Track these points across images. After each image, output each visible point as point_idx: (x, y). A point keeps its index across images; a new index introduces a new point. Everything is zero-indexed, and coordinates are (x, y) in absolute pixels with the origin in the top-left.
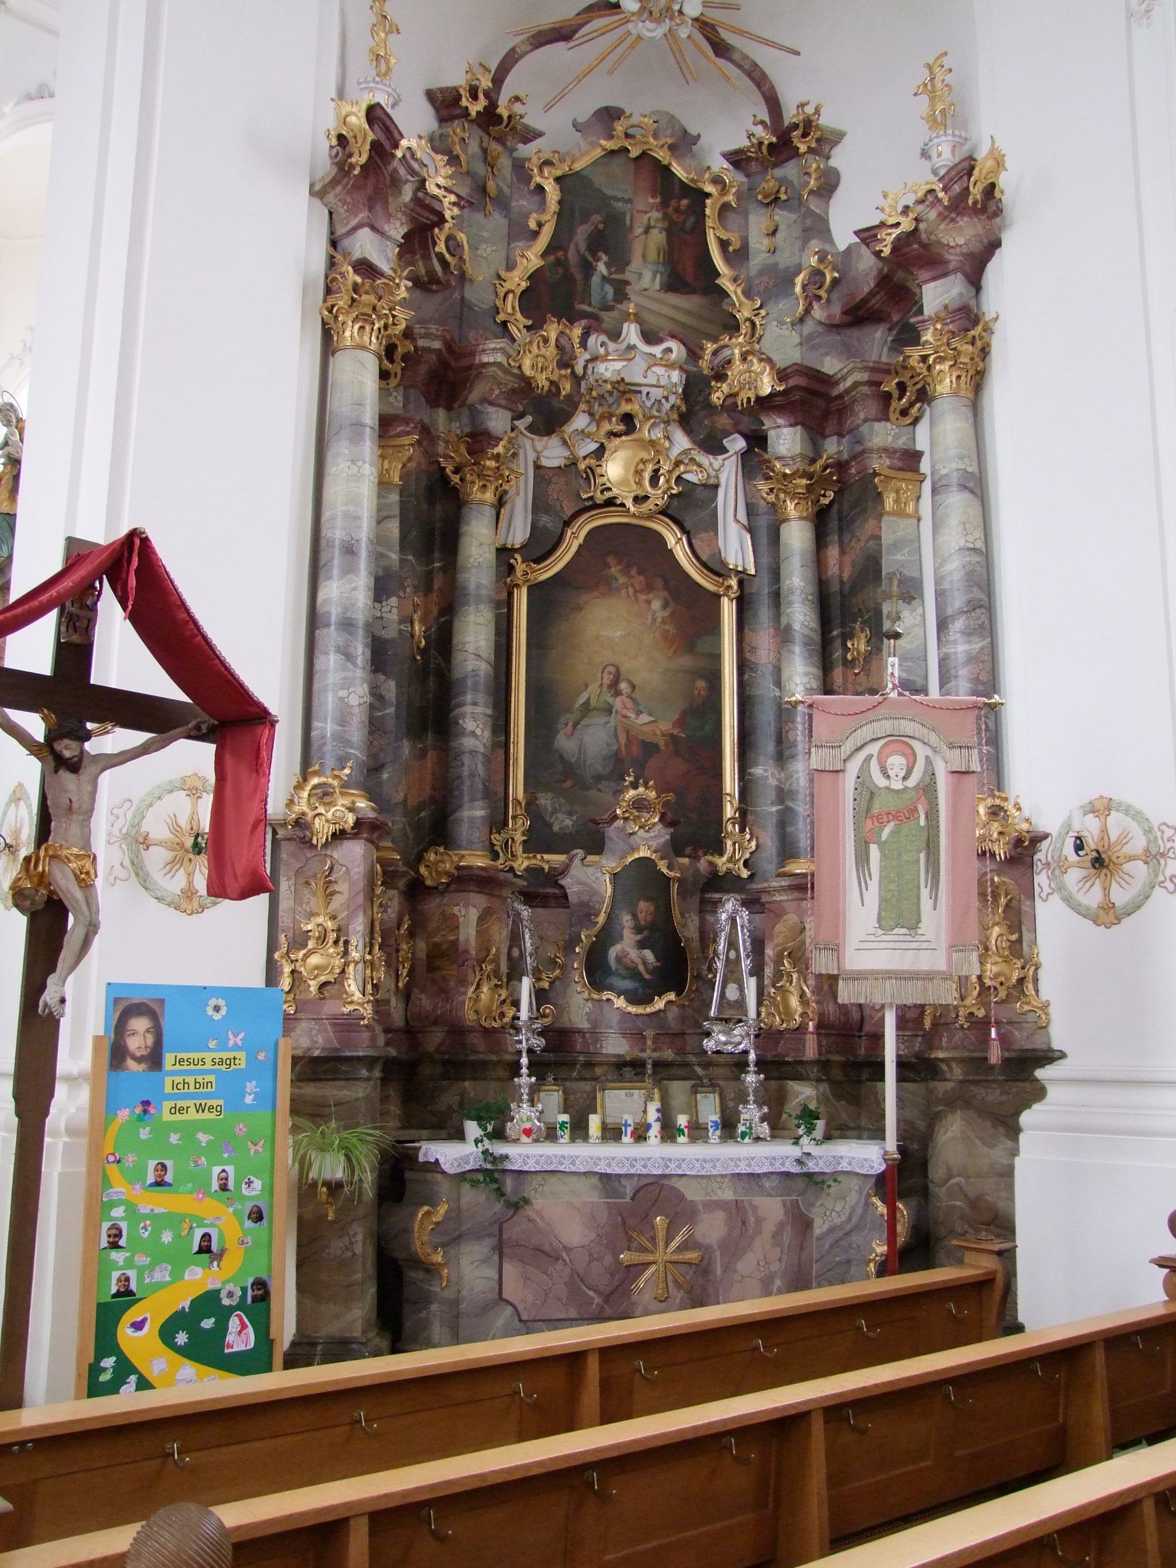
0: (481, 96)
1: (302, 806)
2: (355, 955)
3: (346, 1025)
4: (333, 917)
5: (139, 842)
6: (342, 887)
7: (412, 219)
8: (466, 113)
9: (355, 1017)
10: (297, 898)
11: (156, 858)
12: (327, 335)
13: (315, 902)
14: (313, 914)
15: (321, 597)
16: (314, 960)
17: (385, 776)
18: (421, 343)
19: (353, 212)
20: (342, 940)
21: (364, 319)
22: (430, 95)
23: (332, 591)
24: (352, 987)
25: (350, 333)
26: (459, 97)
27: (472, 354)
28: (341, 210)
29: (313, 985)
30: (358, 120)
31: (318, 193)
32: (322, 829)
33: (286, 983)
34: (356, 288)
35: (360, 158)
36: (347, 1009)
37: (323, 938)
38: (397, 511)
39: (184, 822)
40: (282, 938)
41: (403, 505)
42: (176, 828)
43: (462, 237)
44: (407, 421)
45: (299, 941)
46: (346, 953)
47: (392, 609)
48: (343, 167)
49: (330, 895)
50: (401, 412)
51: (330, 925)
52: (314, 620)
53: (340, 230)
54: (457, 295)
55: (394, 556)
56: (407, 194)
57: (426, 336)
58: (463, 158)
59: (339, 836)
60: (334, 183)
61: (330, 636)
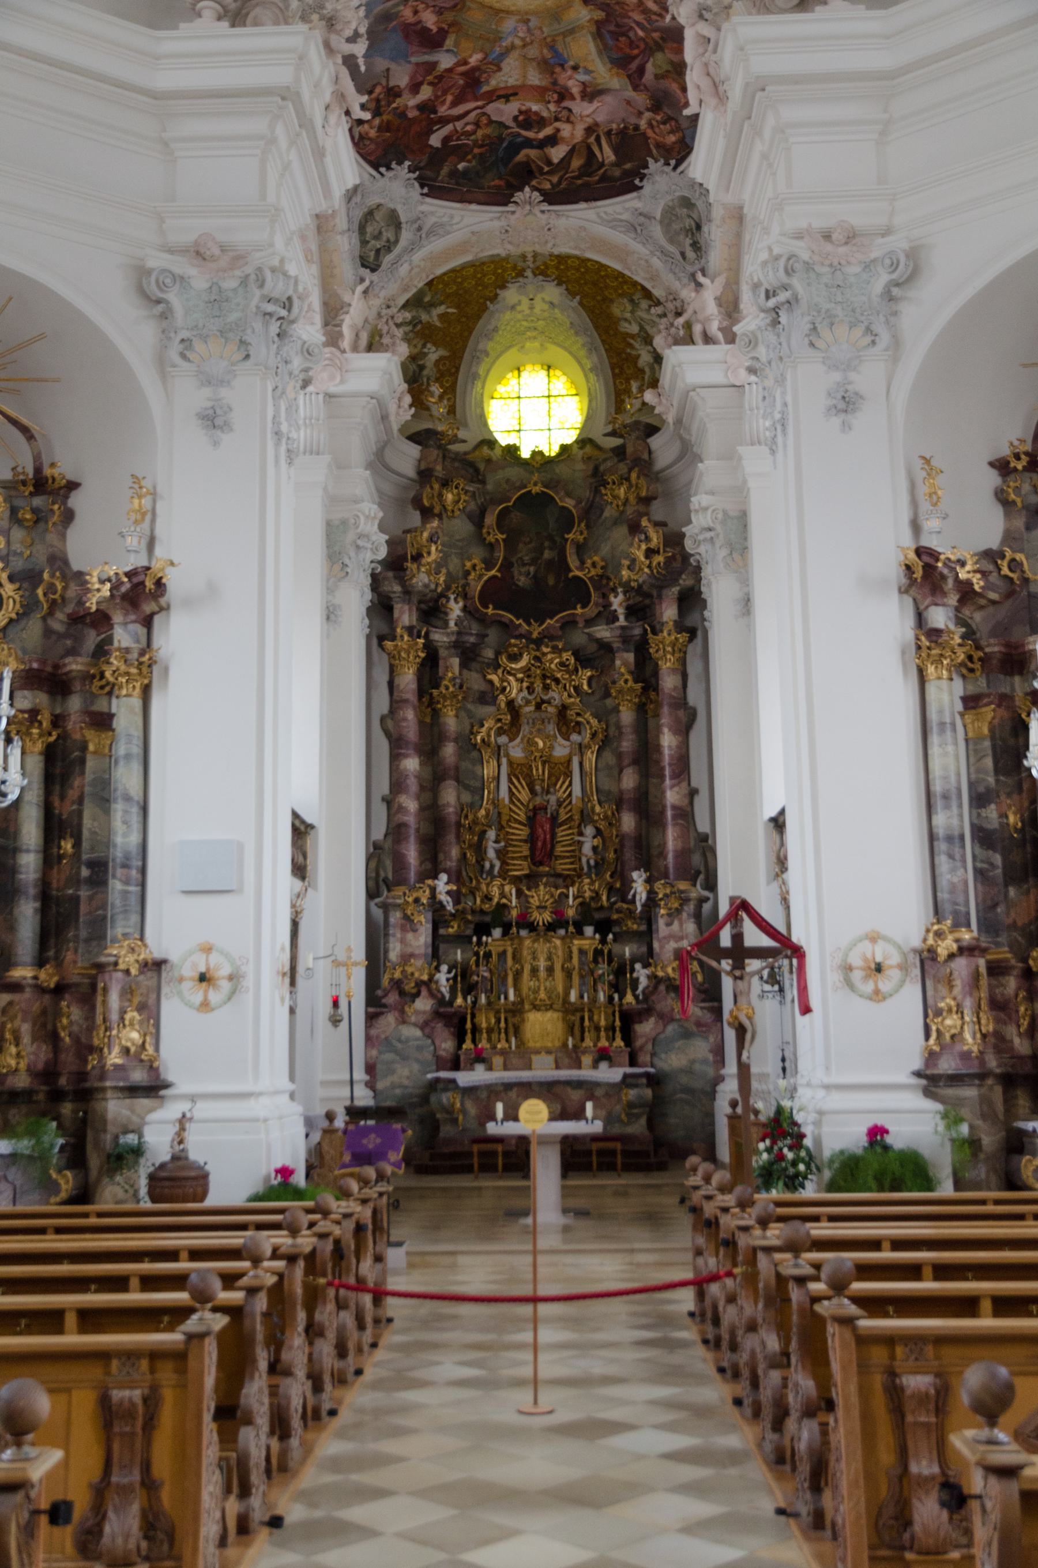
0: (1023, 457)
1: (930, 941)
2: (967, 1019)
3: (965, 1056)
4: (954, 999)
5: (848, 969)
6: (958, 983)
7: (959, 591)
8: (1015, 470)
9: (970, 1052)
10: (936, 990)
11: (857, 976)
12: (921, 672)
13: (943, 990)
14: (943, 998)
15: (934, 822)
16: (948, 1022)
17: (999, 910)
18: (987, 650)
19: (925, 597)
20: (960, 1011)
21: (938, 661)
22: (991, 464)
23: (940, 820)
24: (968, 1036)
25: (931, 669)
26: (1008, 463)
27: (1023, 645)
28: (919, 597)
29: (948, 1036)
30: (912, 555)
31: (903, 591)
32: (942, 952)
33: (934, 1035)
34: (929, 648)
35: (919, 574)
36: (966, 1048)
37: (950, 1011)
38: (990, 752)
39: (869, 956)
40: (930, 1012)
41: (994, 747)
42: (866, 960)
43: (1019, 557)
44: (988, 695)
45: (939, 1013)
46: (962, 1018)
47: (991, 813)
48: (912, 582)
49: (951, 987)
50: (986, 691)
51: (953, 1003)
52: (932, 837)
53: (922, 607)
54: (1025, 593)
55: (991, 780)
56: (950, 582)
57: (989, 645)
58: (1018, 501)
59: (951, 956)
60: (910, 586)
61: (942, 846)
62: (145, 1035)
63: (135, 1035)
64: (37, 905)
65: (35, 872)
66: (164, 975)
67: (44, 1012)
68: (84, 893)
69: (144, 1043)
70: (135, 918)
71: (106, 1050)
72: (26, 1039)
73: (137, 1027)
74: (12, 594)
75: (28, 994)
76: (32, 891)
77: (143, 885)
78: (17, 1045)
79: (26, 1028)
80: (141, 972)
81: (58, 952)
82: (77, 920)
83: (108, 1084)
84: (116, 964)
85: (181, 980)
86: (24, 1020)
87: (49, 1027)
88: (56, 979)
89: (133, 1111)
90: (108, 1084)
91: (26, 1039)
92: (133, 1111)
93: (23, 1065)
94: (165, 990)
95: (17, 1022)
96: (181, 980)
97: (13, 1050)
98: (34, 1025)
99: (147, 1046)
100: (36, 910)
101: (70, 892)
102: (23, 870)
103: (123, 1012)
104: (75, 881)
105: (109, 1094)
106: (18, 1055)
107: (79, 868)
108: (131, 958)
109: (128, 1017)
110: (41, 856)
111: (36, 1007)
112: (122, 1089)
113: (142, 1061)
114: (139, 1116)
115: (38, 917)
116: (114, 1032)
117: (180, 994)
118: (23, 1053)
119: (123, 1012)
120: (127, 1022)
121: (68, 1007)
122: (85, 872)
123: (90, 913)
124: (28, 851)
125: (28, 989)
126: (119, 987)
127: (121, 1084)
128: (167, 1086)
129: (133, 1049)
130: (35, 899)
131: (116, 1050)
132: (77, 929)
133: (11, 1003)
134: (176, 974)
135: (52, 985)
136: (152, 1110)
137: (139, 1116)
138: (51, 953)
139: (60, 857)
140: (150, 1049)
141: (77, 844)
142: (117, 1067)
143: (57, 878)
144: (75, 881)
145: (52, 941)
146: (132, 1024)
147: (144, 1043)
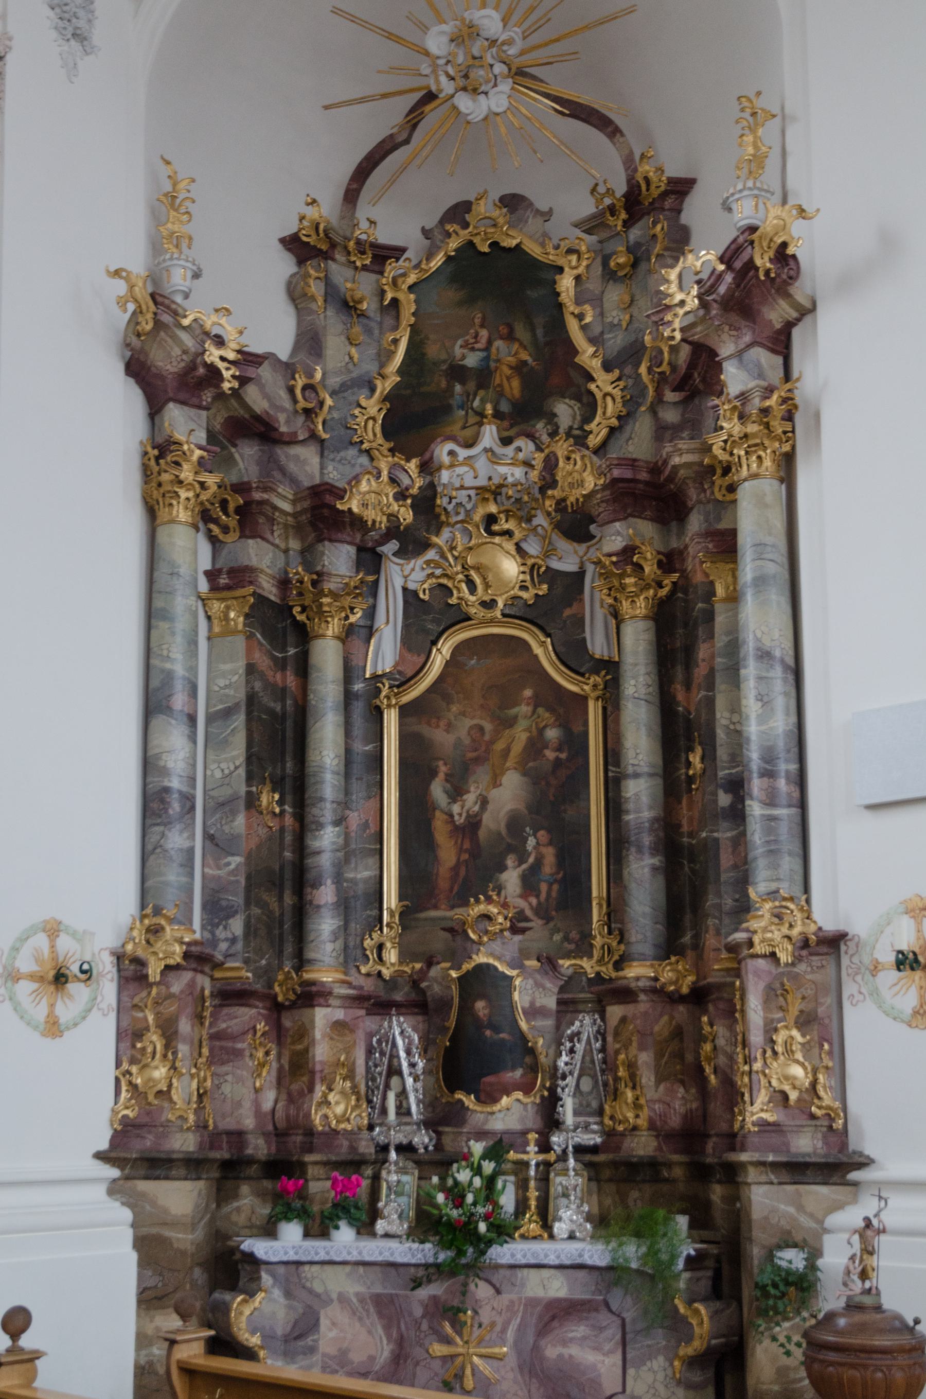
62: (815, 1071)
63: (797, 1071)
64: (656, 861)
65: (651, 808)
66: (845, 961)
67: (678, 1033)
68: (724, 834)
69: (814, 1084)
70: (789, 864)
71: (747, 1097)
72: (647, 1077)
73: (799, 1056)
74: (609, 389)
75: (644, 1004)
76: (647, 840)
77: (802, 805)
78: (634, 1088)
79: (645, 1058)
80: (798, 959)
81: (697, 937)
82: (717, 880)
83: (744, 1157)
84: (750, 944)
85: (876, 968)
86: (642, 1047)
87: (689, 1057)
88: (691, 979)
89: (800, 1208)
90: (744, 1157)
91: (647, 1077)
92: (800, 1208)
93: (642, 1122)
94: (849, 988)
95: (633, 1050)
96: (876, 968)
97: (630, 1095)
98: (659, 1055)
99: (822, 1093)
100: (654, 869)
101: (704, 835)
102: (631, 806)
103: (770, 1030)
104: (712, 816)
105: (752, 1175)
106: (637, 1106)
107: (715, 794)
108: (776, 935)
109: (780, 1038)
110: (659, 781)
111: (662, 1026)
112: (774, 1166)
113: (813, 1117)
114: (812, 1216)
115: (661, 881)
116: (757, 1066)
117: (875, 993)
118: (642, 1101)
119: (770, 1030)
120: (779, 1049)
121: (711, 1025)
122: (724, 799)
123: (735, 867)
124: (636, 776)
125: (642, 997)
126: (762, 985)
127: (771, 1158)
128: (864, 1163)
129: (793, 1096)
130: (654, 851)
131: (762, 1097)
132: (719, 895)
133: (623, 1020)
134: (867, 960)
135: (685, 990)
136: (838, 1206)
137: (812, 1216)
138: (687, 939)
139: (690, 780)
140: (828, 1098)
141: (709, 756)
142: (764, 1125)
143: (685, 815)
144: (712, 816)
145: (688, 917)
146: (789, 1051)
147: (814, 1084)
